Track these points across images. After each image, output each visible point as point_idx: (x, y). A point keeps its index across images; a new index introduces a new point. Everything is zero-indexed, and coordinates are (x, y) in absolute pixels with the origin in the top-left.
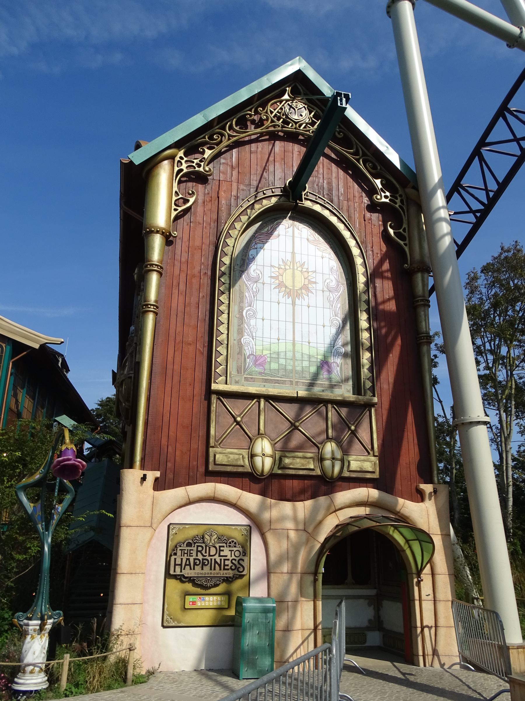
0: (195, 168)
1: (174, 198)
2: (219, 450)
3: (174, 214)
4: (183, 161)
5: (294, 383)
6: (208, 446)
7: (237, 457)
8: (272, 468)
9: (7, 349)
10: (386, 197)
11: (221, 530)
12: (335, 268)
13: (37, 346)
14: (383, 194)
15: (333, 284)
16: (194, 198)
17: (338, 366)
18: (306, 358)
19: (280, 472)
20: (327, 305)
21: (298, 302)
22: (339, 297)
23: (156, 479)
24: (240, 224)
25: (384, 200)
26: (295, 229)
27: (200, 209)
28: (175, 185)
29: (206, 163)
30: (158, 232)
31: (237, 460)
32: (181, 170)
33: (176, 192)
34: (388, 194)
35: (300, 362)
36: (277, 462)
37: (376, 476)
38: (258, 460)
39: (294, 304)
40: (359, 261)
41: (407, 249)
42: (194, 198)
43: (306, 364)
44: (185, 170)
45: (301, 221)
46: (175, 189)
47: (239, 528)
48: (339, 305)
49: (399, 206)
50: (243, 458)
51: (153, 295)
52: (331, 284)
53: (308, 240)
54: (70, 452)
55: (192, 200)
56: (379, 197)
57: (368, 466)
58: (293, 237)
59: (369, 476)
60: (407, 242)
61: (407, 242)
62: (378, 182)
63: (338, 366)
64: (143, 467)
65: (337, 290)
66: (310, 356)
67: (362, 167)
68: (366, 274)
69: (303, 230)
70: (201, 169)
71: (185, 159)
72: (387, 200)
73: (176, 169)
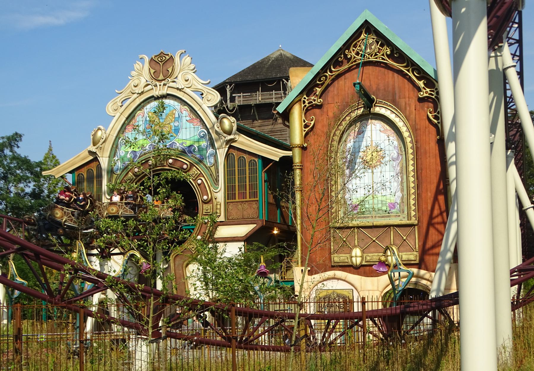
0: (312, 102)
1: (304, 124)
2: (336, 255)
3: (304, 133)
4: (306, 100)
5: (374, 217)
6: (330, 253)
7: (344, 258)
8: (361, 262)
9: (259, 162)
10: (426, 92)
11: (339, 292)
12: (396, 145)
13: (277, 159)
14: (424, 91)
15: (395, 155)
16: (313, 121)
17: (398, 204)
18: (380, 202)
19: (366, 264)
20: (392, 169)
21: (374, 171)
22: (399, 163)
23: (309, 271)
24: (339, 131)
25: (425, 95)
26: (373, 125)
27: (319, 126)
28: (303, 116)
29: (318, 97)
30: (296, 147)
31: (344, 260)
32: (305, 106)
33: (304, 120)
34: (428, 90)
35: (376, 205)
36: (364, 259)
37: (417, 262)
38: (354, 259)
39: (373, 172)
40: (409, 140)
41: (439, 125)
42: (313, 121)
43: (380, 206)
44: (308, 105)
45: (376, 119)
46: (304, 118)
47: (347, 290)
48: (399, 168)
49: (435, 97)
50: (347, 258)
51: (298, 182)
52: (394, 156)
53: (380, 130)
54: (263, 267)
55: (312, 123)
56: (422, 93)
57: (412, 257)
58: (371, 130)
59: (413, 262)
60: (440, 121)
61: (440, 121)
62: (421, 84)
63: (398, 204)
64: (302, 265)
65: (397, 159)
66: (382, 201)
67: (411, 74)
68: (413, 147)
69: (377, 124)
70: (316, 102)
71: (307, 98)
72: (427, 95)
73: (303, 105)
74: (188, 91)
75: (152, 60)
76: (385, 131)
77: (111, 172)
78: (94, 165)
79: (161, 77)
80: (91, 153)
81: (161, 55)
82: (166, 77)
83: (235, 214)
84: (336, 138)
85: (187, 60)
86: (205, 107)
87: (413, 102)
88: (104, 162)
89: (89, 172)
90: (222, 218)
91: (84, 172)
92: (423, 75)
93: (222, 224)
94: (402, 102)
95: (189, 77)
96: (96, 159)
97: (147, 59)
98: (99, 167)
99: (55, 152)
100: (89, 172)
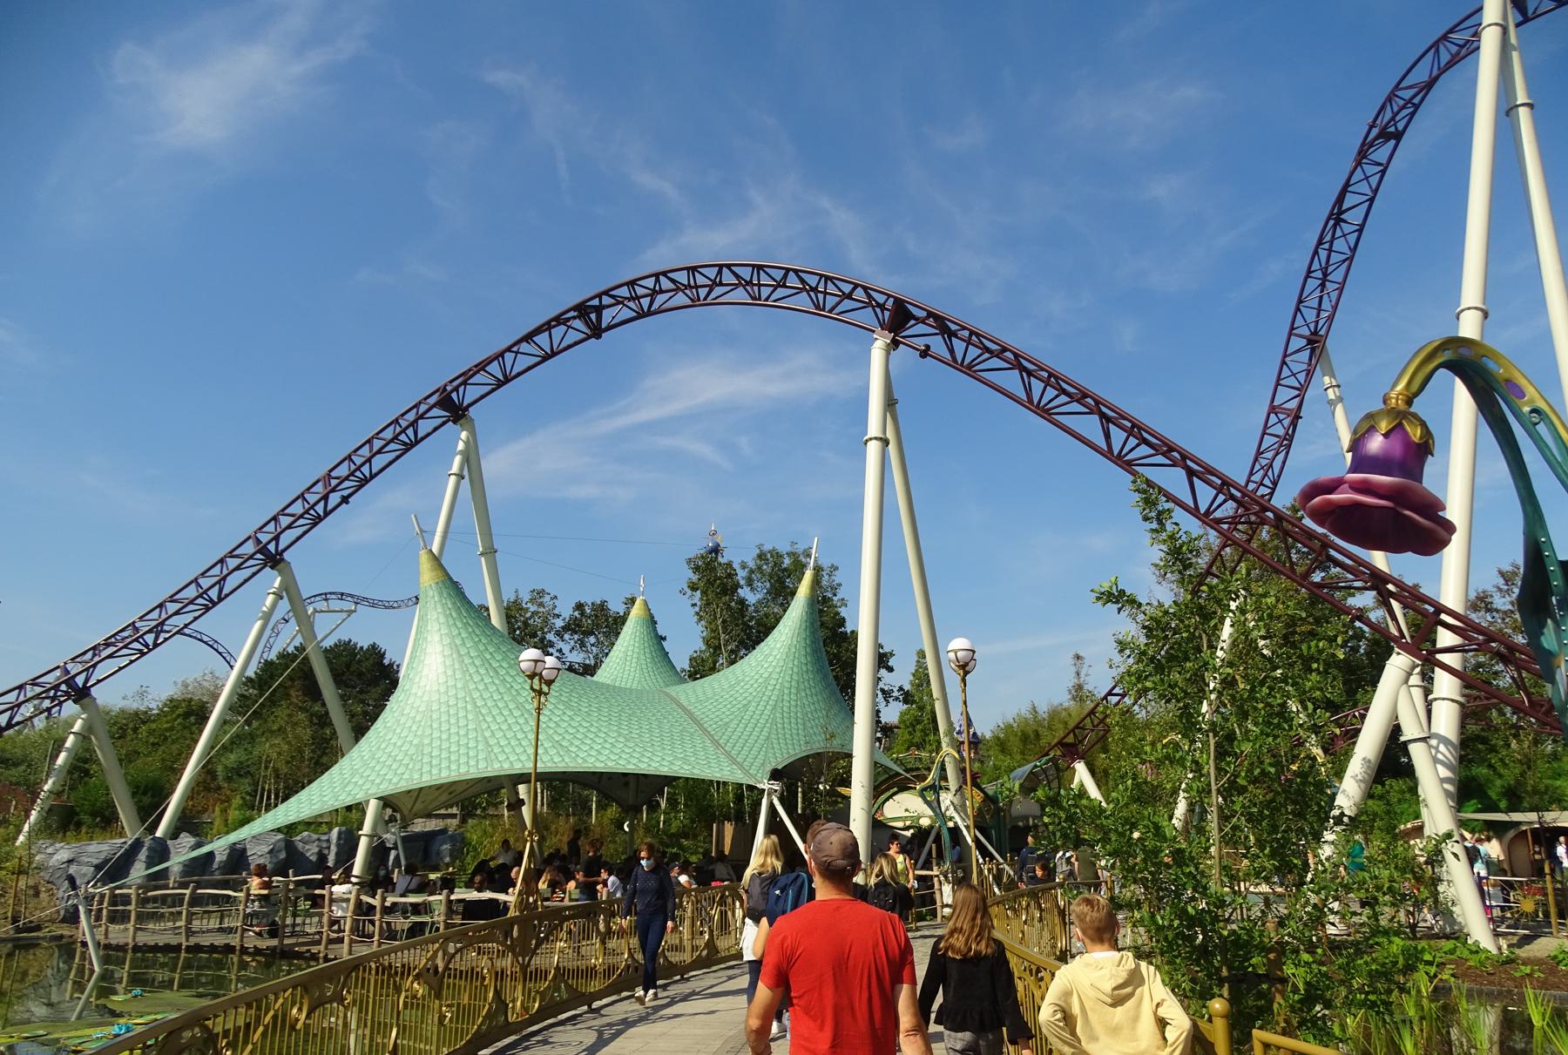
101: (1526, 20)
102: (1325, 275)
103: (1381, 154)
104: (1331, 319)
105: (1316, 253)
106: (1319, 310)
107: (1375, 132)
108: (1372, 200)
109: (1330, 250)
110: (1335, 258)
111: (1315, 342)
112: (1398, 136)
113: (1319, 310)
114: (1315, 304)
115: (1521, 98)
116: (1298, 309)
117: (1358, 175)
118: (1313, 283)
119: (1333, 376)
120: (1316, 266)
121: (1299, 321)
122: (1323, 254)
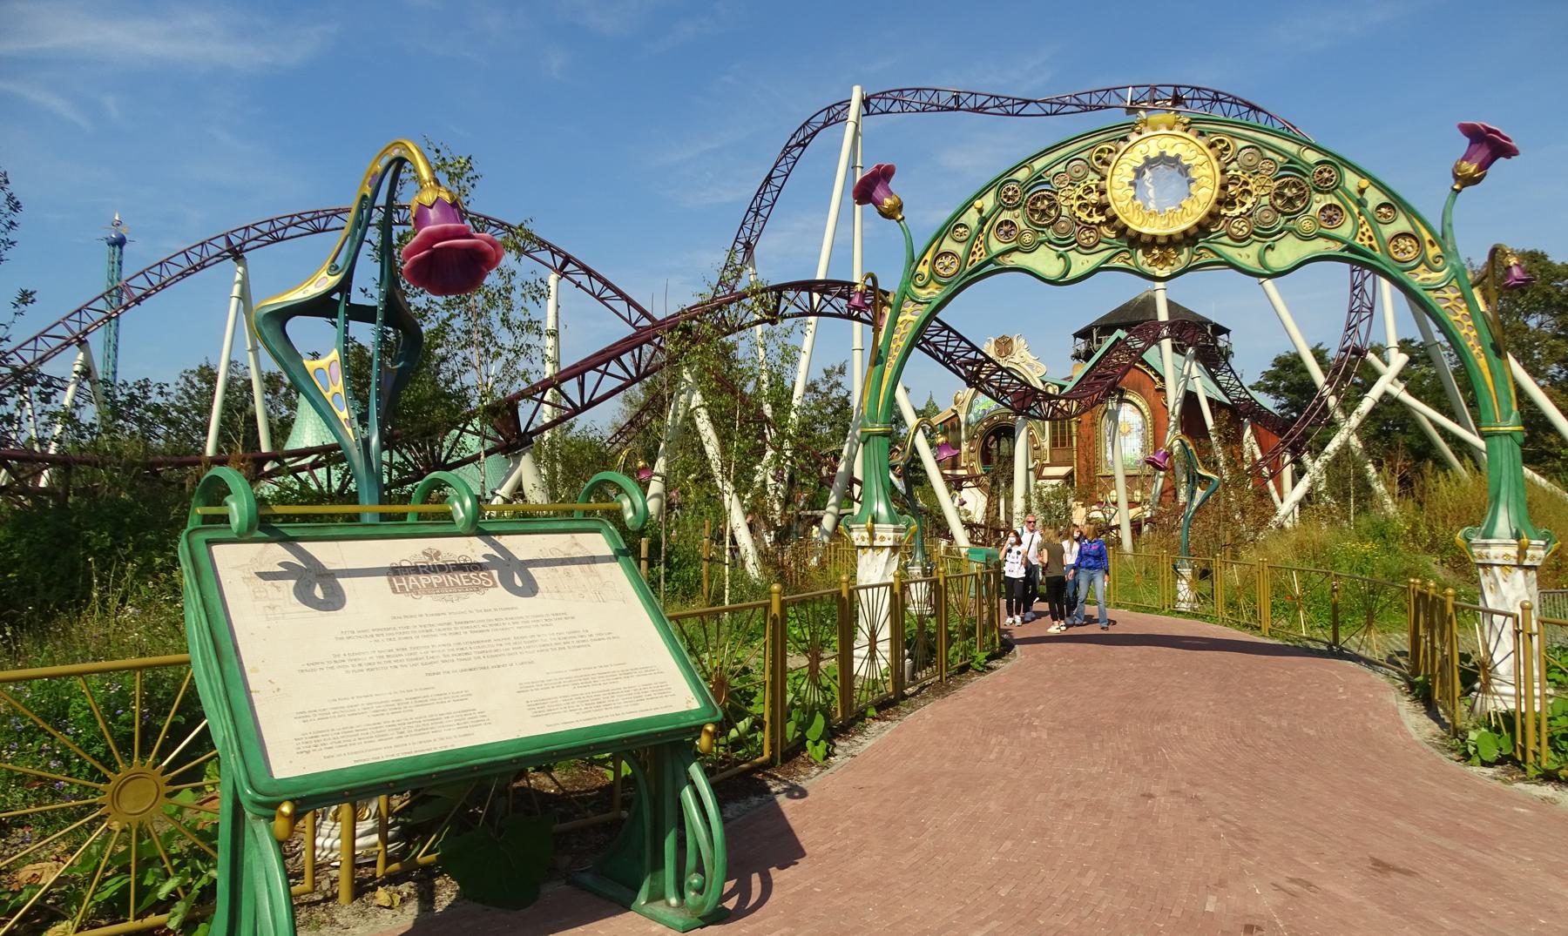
74: (1023, 365)
75: (996, 342)
76: (1133, 411)
77: (968, 424)
78: (955, 419)
79: (1003, 354)
80: (953, 410)
81: (1003, 337)
82: (1007, 354)
83: (1057, 459)
84: (1100, 415)
85: (1022, 341)
86: (1035, 377)
87: (1153, 391)
88: (962, 417)
89: (953, 425)
90: (1048, 461)
91: (948, 424)
92: (1157, 374)
93: (1048, 465)
94: (1145, 391)
95: (1023, 354)
96: (956, 415)
97: (993, 340)
98: (959, 420)
99: (934, 400)
100: (953, 425)
101: (868, 114)
102: (758, 209)
103: (796, 153)
104: (758, 236)
105: (755, 198)
106: (752, 230)
107: (793, 142)
108: (787, 175)
109: (762, 198)
110: (764, 203)
111: (748, 247)
112: (805, 146)
113: (752, 230)
114: (750, 226)
115: (859, 164)
116: (741, 228)
117: (783, 161)
118: (751, 214)
119: (754, 268)
120: (755, 205)
121: (741, 235)
122: (759, 199)
